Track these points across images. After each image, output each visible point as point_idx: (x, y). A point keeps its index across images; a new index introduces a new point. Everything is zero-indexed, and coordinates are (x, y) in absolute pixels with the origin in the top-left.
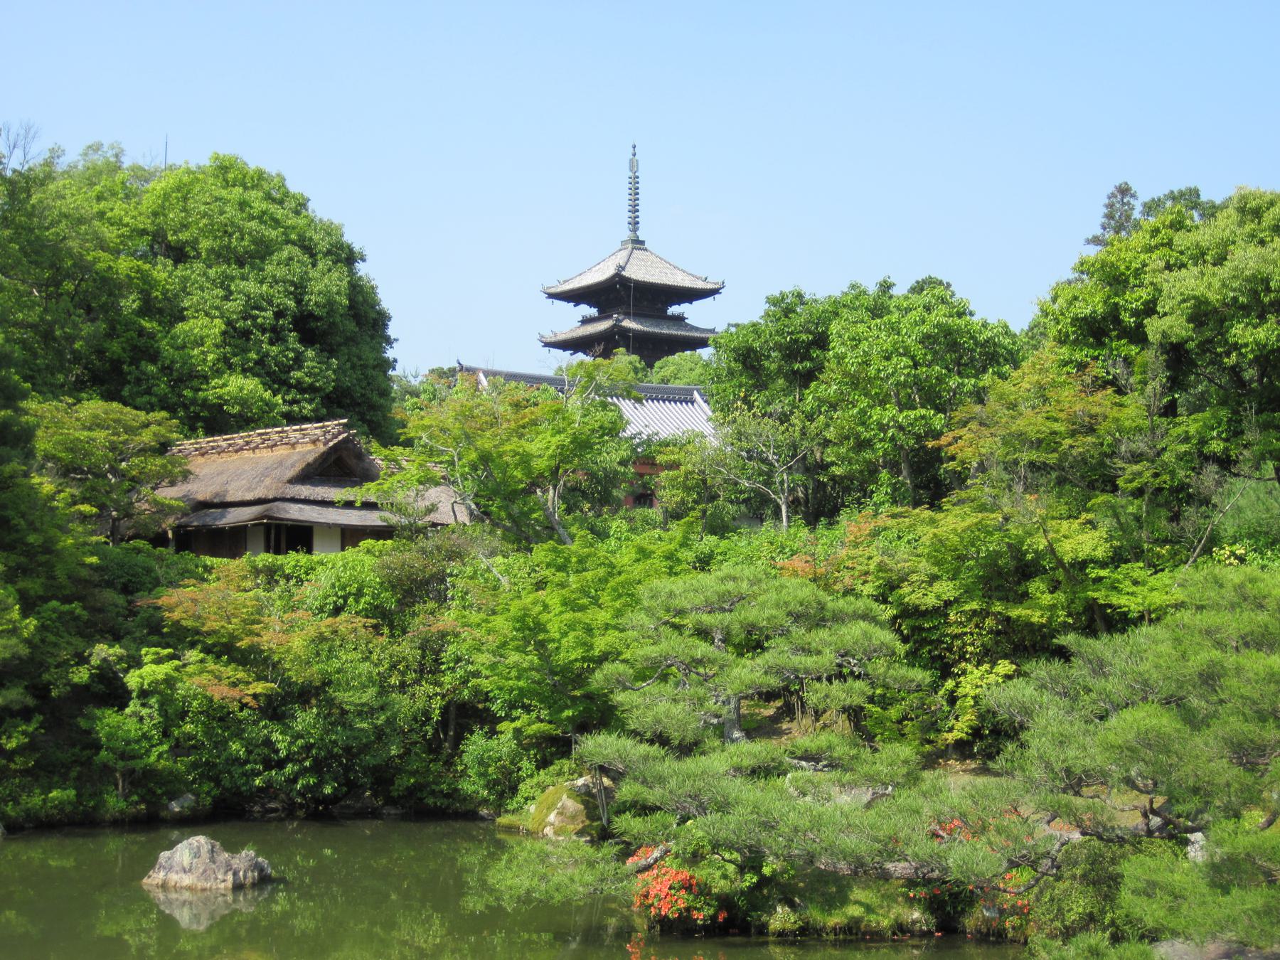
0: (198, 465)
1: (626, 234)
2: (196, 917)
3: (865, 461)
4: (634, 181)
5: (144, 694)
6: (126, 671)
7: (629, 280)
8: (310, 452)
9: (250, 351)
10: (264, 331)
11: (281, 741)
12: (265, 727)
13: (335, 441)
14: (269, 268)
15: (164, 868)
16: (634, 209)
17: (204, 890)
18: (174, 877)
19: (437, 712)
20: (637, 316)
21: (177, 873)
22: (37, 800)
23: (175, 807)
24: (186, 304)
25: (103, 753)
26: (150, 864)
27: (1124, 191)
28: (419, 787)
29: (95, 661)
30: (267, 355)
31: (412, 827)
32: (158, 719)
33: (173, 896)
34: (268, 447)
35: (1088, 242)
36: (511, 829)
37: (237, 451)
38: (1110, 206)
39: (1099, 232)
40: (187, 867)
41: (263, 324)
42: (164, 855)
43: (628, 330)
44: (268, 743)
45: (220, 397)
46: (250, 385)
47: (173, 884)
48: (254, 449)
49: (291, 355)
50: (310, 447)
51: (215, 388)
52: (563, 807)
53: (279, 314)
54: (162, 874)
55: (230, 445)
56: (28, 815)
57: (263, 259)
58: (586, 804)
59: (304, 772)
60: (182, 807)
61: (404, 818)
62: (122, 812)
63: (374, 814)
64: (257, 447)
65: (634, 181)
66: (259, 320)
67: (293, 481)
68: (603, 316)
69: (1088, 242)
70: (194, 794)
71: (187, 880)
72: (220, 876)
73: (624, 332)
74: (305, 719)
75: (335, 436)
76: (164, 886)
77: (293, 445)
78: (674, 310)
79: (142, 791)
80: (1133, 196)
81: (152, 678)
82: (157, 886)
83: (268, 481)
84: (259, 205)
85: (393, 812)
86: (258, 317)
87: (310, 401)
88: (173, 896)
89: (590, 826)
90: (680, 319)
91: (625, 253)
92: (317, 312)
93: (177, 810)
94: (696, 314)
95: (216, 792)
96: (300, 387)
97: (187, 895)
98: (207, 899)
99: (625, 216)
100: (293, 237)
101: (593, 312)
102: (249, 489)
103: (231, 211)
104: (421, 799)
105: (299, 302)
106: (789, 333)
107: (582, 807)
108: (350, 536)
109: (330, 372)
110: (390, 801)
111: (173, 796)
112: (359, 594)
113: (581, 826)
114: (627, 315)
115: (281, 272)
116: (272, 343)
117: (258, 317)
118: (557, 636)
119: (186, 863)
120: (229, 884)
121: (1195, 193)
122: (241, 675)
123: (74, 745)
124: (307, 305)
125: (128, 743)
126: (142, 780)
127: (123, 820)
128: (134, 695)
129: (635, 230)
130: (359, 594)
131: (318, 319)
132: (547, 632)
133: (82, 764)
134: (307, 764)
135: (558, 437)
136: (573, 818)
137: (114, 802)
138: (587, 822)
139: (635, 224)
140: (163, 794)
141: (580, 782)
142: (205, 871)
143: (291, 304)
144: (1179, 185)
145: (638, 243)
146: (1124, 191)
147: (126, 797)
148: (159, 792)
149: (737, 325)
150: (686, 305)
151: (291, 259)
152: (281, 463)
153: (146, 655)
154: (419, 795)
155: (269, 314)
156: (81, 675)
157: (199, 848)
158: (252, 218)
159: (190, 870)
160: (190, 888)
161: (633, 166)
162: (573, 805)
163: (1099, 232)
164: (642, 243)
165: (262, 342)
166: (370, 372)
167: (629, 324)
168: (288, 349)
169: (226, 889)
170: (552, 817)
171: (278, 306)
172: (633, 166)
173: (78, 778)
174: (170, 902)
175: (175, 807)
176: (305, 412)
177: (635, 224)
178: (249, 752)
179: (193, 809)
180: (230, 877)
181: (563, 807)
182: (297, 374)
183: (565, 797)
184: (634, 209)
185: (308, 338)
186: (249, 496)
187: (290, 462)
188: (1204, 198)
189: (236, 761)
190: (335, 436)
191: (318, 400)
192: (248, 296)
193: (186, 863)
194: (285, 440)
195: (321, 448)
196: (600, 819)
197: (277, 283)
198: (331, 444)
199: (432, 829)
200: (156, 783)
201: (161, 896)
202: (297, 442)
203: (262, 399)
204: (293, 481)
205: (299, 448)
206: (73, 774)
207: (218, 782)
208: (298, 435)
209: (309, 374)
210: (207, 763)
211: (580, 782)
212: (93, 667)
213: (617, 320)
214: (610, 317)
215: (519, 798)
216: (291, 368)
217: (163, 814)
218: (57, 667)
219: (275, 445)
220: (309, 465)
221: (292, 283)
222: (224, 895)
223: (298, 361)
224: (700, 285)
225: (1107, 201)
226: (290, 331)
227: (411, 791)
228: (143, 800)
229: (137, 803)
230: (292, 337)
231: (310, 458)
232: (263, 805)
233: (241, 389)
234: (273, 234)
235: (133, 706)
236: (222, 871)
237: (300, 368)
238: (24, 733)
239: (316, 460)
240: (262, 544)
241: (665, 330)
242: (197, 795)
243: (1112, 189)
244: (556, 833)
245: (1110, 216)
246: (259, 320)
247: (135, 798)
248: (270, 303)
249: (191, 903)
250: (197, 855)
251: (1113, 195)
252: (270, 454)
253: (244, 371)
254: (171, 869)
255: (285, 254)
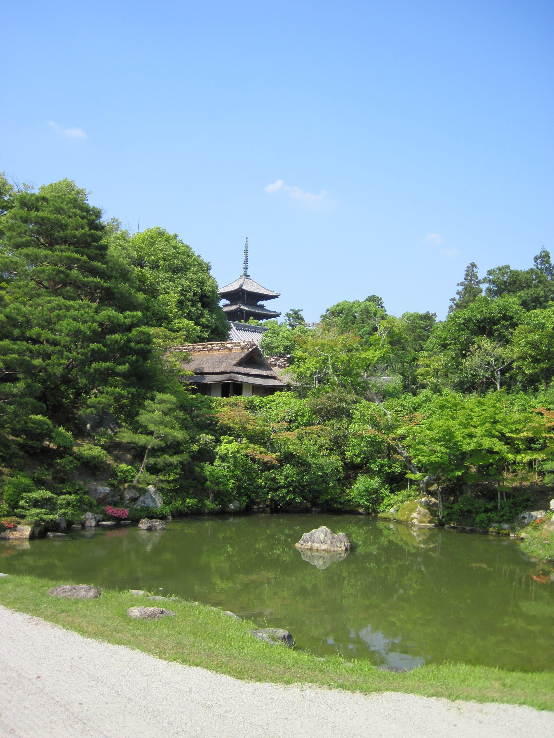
0: (195, 355)
1: (243, 272)
2: (325, 563)
3: (541, 368)
4: (247, 251)
5: (223, 459)
6: (215, 446)
7: (244, 290)
8: (241, 353)
9: (184, 309)
10: (189, 301)
11: (280, 479)
12: (273, 472)
13: (252, 349)
14: (189, 275)
15: (310, 541)
16: (246, 263)
17: (334, 551)
18: (316, 545)
19: (341, 468)
20: (247, 305)
21: (317, 543)
22: (178, 503)
23: (232, 507)
24: (159, 288)
25: (208, 483)
26: (298, 538)
27: (473, 265)
28: (331, 499)
29: (202, 442)
30: (190, 311)
31: (324, 516)
32: (232, 468)
33: (316, 554)
34: (217, 350)
35: (458, 284)
36: (386, 519)
37: (199, 351)
38: (467, 271)
39: (463, 280)
40: (323, 541)
41: (188, 298)
42: (306, 535)
43: (244, 310)
44: (274, 479)
45: (178, 328)
46: (192, 323)
47: (316, 548)
48: (209, 351)
49: (200, 312)
50: (241, 351)
51: (176, 323)
52: (419, 511)
53: (195, 294)
54: (310, 544)
55: (194, 348)
56: (177, 510)
57: (186, 271)
58: (429, 509)
59: (289, 492)
60: (235, 507)
61: (322, 512)
62: (213, 509)
63: (306, 511)
64: (210, 350)
65: (247, 251)
66: (187, 296)
67: (235, 365)
68: (232, 303)
69: (458, 284)
70: (238, 501)
71: (323, 547)
72: (338, 545)
73: (242, 310)
74: (288, 469)
75: (251, 347)
76: (311, 549)
77: (231, 350)
78: (260, 303)
79: (219, 500)
80: (476, 268)
81: (232, 450)
82: (307, 549)
83: (224, 365)
84: (182, 249)
85: (317, 510)
86: (186, 295)
87: (207, 331)
88: (316, 554)
89: (433, 519)
90: (262, 307)
91: (242, 280)
92: (209, 294)
93: (233, 508)
94: (269, 305)
95: (247, 501)
96: (204, 326)
97: (323, 553)
98: (334, 555)
99: (242, 265)
100: (196, 263)
101: (228, 302)
102: (215, 367)
103: (171, 251)
104: (331, 505)
105: (201, 289)
106: (492, 313)
107: (427, 511)
108: (271, 390)
109: (213, 320)
110: (314, 504)
111: (230, 502)
112: (303, 415)
113: (429, 519)
114: (243, 304)
115: (194, 277)
116: (192, 306)
117: (186, 295)
118: (461, 439)
119: (322, 539)
120: (344, 549)
121: (508, 267)
122: (263, 449)
123: (188, 479)
124: (205, 291)
125: (218, 478)
126: (220, 496)
127: (212, 513)
128: (218, 457)
129: (246, 271)
130: (303, 415)
131: (208, 297)
132: (455, 437)
133: (192, 487)
134: (291, 489)
135: (378, 352)
136: (425, 515)
137: (209, 504)
138: (431, 517)
139: (246, 268)
140: (227, 501)
141: (423, 500)
142: (332, 543)
143: (200, 291)
144: (502, 264)
145: (247, 276)
146: (473, 265)
147: (213, 502)
148: (226, 500)
149: (293, 310)
150: (265, 301)
151: (198, 271)
152: (227, 357)
153: (223, 439)
154: (330, 503)
155: (192, 294)
156: (195, 447)
157: (326, 532)
158: (179, 253)
159: (324, 542)
160: (325, 550)
161: (246, 246)
162: (424, 510)
163: (463, 280)
164: (249, 276)
165: (188, 306)
166: (224, 321)
167: (243, 307)
168: (198, 309)
169: (342, 551)
170: (415, 515)
171: (194, 290)
172: (246, 246)
173: (193, 494)
174: (313, 557)
175: (232, 507)
176: (206, 336)
177: (246, 268)
178: (266, 484)
179: (239, 508)
180: (343, 545)
181: (419, 511)
182: (204, 320)
183: (419, 506)
184: (246, 263)
185: (203, 306)
186: (217, 370)
187: (231, 357)
188: (511, 268)
189: (261, 487)
190: (251, 347)
191: (210, 331)
192: (183, 285)
193: (322, 539)
194: (225, 347)
195: (246, 352)
196: (438, 516)
197: (192, 281)
198: (250, 350)
199: (336, 518)
200: (224, 496)
201: (309, 554)
202: (232, 349)
203: (195, 329)
204: (235, 365)
205: (233, 351)
206: (191, 492)
207: (249, 497)
208: (210, 346)
209: (207, 320)
210: (245, 487)
211: (423, 500)
212: (200, 444)
213: (240, 306)
214: (237, 304)
215: (382, 505)
216: (198, 318)
217: (226, 510)
218: (185, 444)
219: (220, 349)
220: (242, 358)
221: (199, 282)
222: (341, 554)
223: (202, 315)
224: (271, 294)
225: (466, 269)
226: (199, 302)
227: (327, 501)
228: (219, 504)
229: (217, 505)
230: (199, 304)
231: (243, 355)
232: (258, 506)
233: (188, 325)
234: (191, 260)
235: (217, 462)
236: (339, 542)
237: (203, 317)
238: (176, 473)
239: (245, 356)
240: (220, 392)
241: (257, 311)
242: (240, 502)
243: (469, 265)
244: (421, 522)
245: (468, 275)
246: (187, 296)
247: (217, 503)
248: (190, 289)
249: (323, 557)
250: (326, 535)
251: (469, 267)
252: (208, 353)
253: (185, 317)
254: (314, 541)
255: (195, 270)
